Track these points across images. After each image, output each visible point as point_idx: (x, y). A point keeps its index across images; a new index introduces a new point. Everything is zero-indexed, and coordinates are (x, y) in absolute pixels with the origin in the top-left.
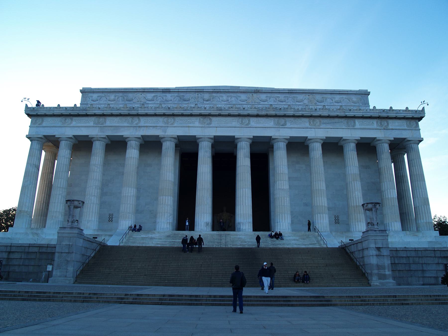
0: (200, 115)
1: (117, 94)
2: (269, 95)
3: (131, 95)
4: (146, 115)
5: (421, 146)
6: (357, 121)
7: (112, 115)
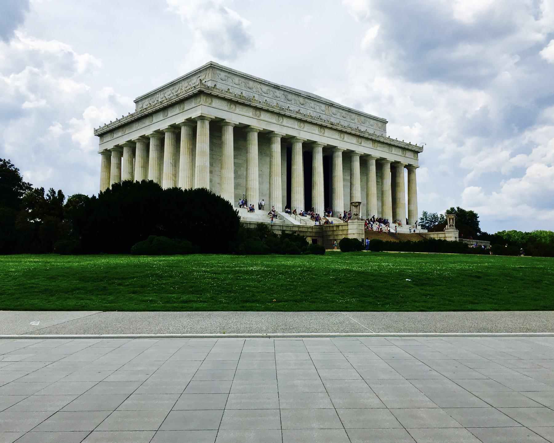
0: (321, 126)
1: (240, 79)
3: (251, 84)
4: (290, 117)
5: (418, 171)
7: (267, 111)
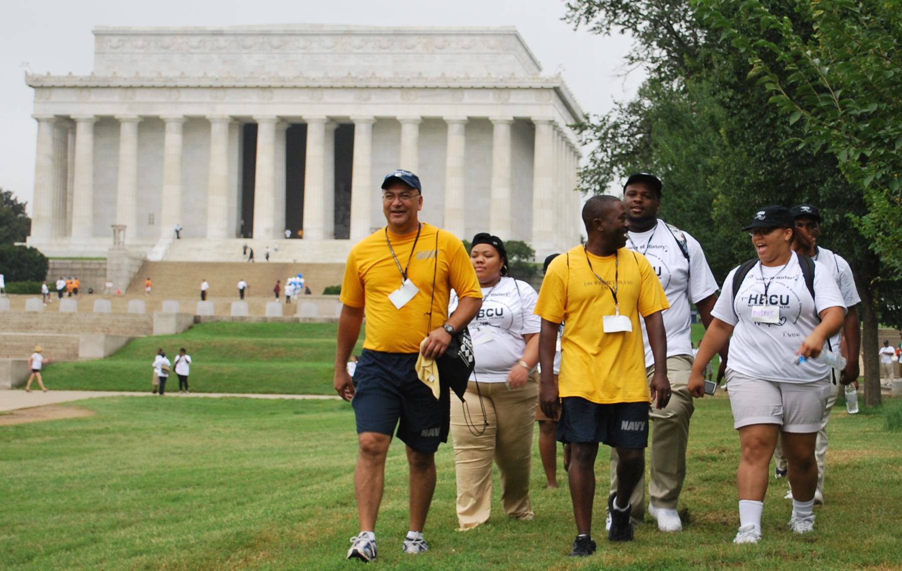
2: (365, 38)
3: (167, 40)
6: (466, 94)
